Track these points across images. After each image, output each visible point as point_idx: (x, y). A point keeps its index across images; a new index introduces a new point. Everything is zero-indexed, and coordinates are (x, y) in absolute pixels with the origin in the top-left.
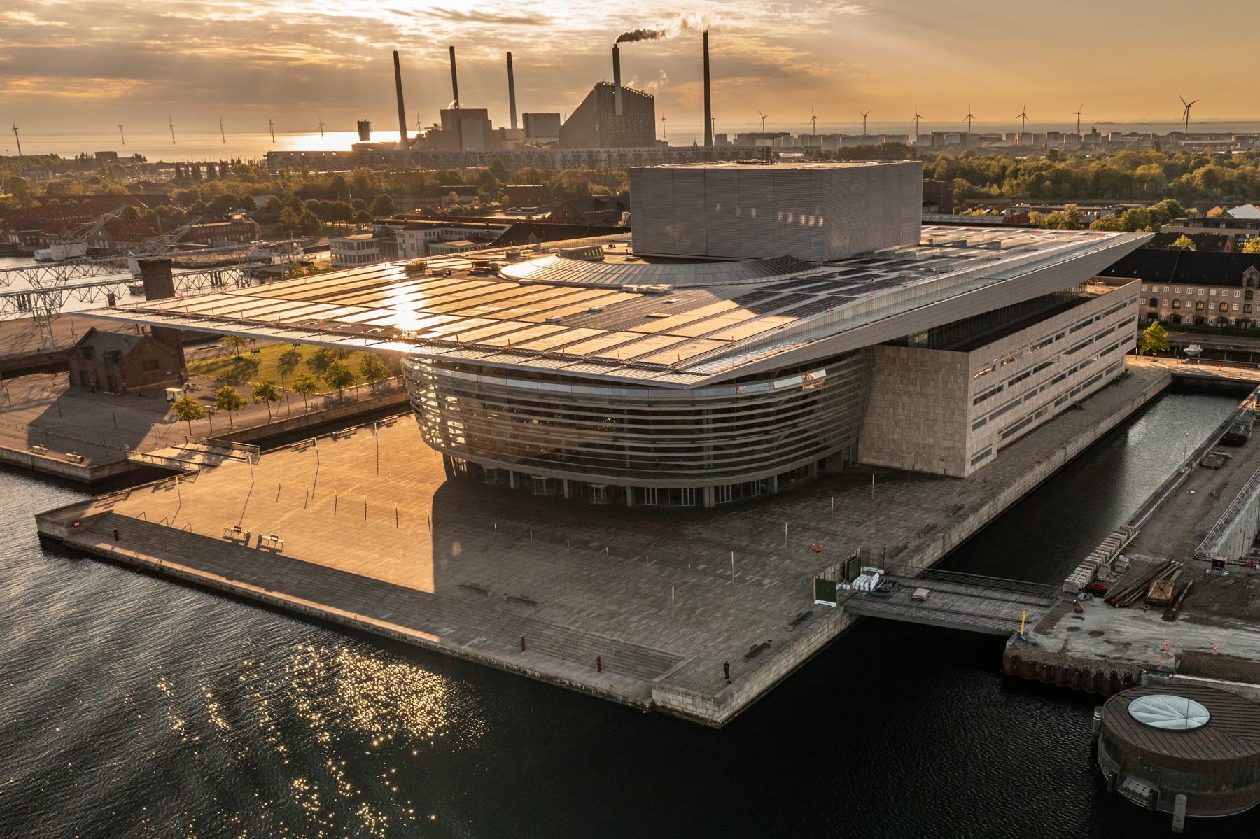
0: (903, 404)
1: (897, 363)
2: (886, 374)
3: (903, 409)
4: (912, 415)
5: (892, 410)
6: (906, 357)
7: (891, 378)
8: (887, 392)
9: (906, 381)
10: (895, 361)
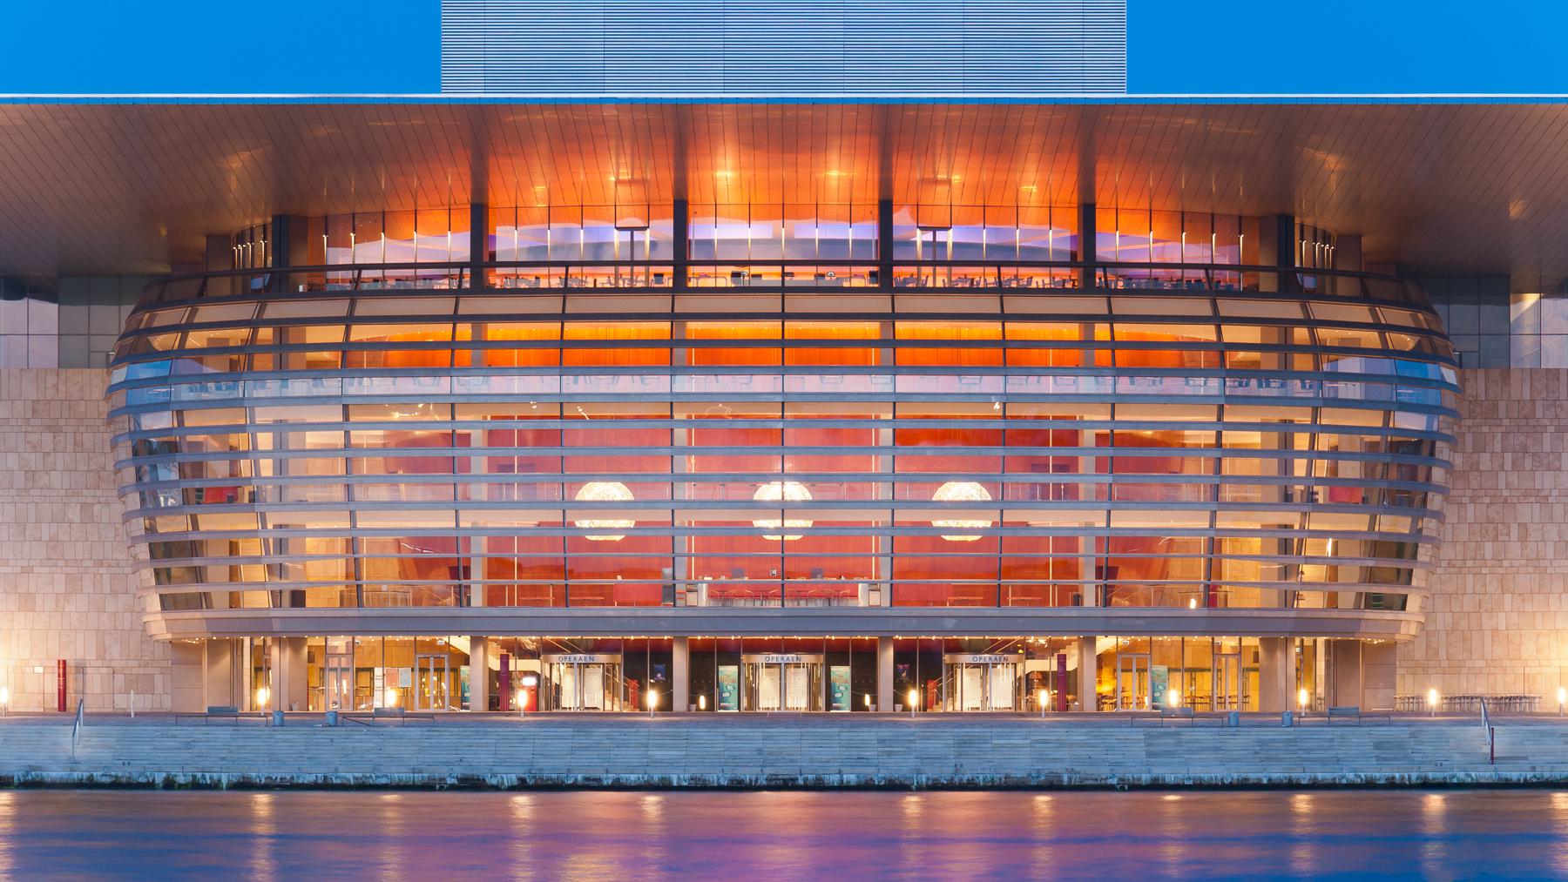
0: (1523, 527)
1: (1502, 413)
2: (1469, 449)
3: (1523, 539)
4: (1550, 555)
5: (1489, 546)
6: (1527, 396)
7: (1485, 461)
8: (1473, 499)
9: (1528, 462)
10: (1495, 407)
